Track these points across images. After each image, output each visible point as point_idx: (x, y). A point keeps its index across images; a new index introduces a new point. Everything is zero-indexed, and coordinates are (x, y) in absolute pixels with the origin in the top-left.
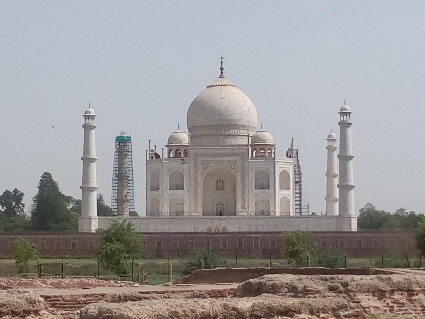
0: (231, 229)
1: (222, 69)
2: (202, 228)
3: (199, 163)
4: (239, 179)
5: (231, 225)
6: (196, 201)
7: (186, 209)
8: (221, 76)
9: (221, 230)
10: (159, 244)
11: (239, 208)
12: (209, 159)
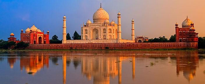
11: (99, 38)
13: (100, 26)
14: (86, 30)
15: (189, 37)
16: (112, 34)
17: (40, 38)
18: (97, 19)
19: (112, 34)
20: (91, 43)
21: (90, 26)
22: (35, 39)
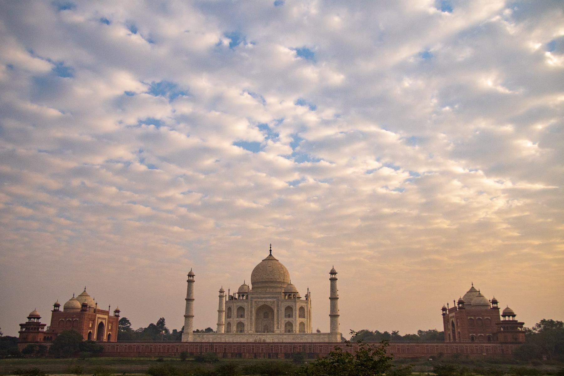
0: (268, 341)
1: (271, 251)
2: (251, 340)
3: (254, 302)
4: (275, 311)
5: (269, 338)
6: (251, 324)
7: (246, 329)
8: (271, 255)
9: (262, 341)
10: (225, 349)
11: (275, 329)
12: (259, 300)
13: (278, 300)
14: (241, 309)
15: (508, 332)
16: (306, 319)
17: (101, 325)
18: (266, 282)
19: (306, 319)
20: (260, 343)
21: (252, 298)
22: (91, 328)
